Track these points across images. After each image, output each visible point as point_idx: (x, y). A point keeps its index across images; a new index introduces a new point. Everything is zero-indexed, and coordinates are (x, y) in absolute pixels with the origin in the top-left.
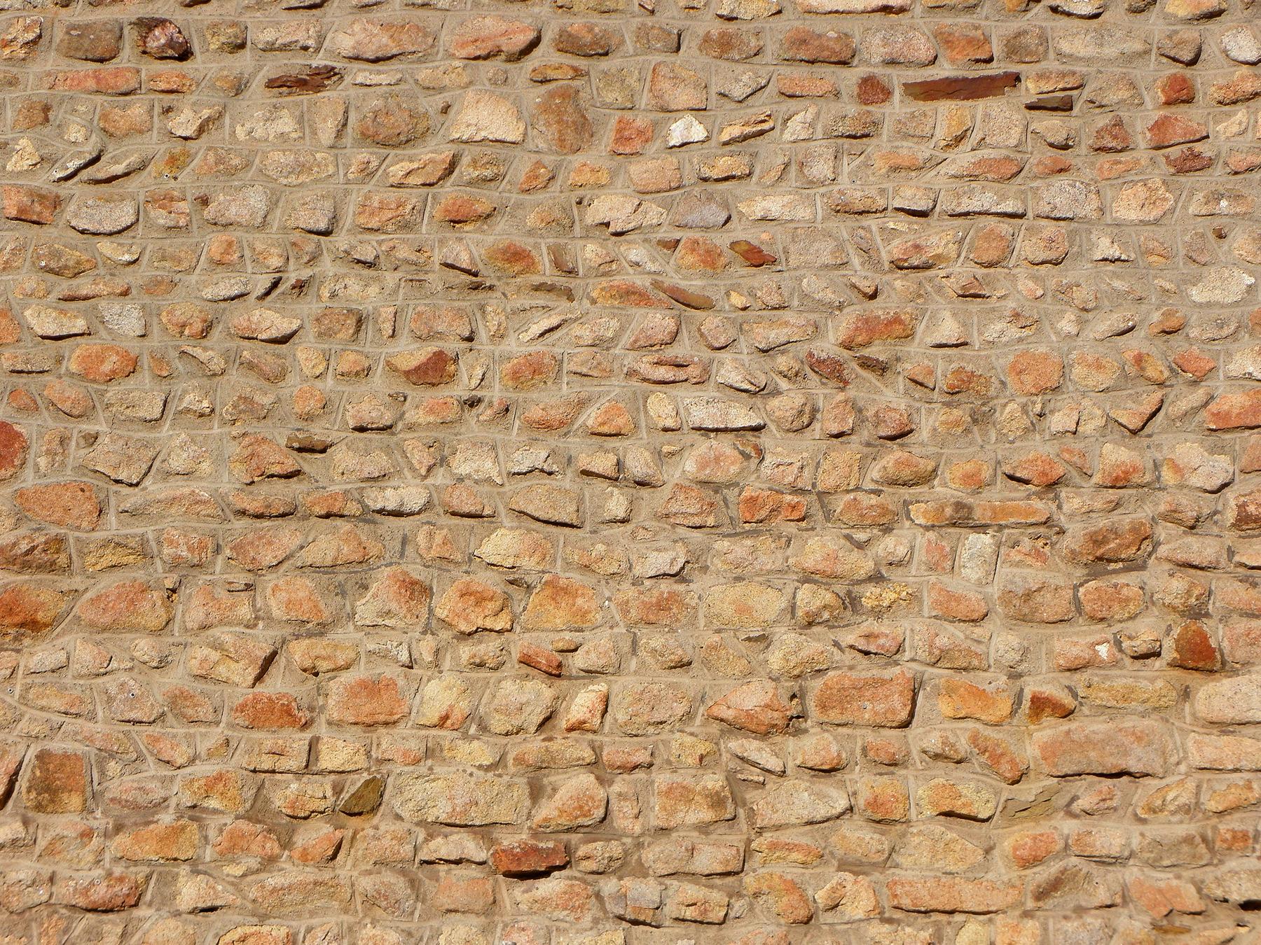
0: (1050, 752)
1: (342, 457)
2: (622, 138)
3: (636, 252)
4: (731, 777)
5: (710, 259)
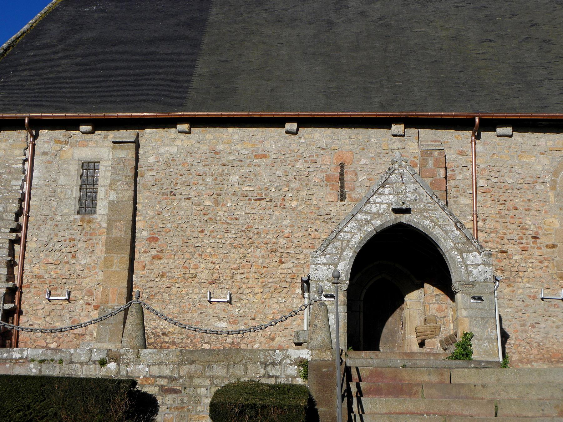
0: (265, 272)
1: (192, 241)
2: (222, 205)
3: (224, 218)
4: (232, 274)
5: (232, 219)
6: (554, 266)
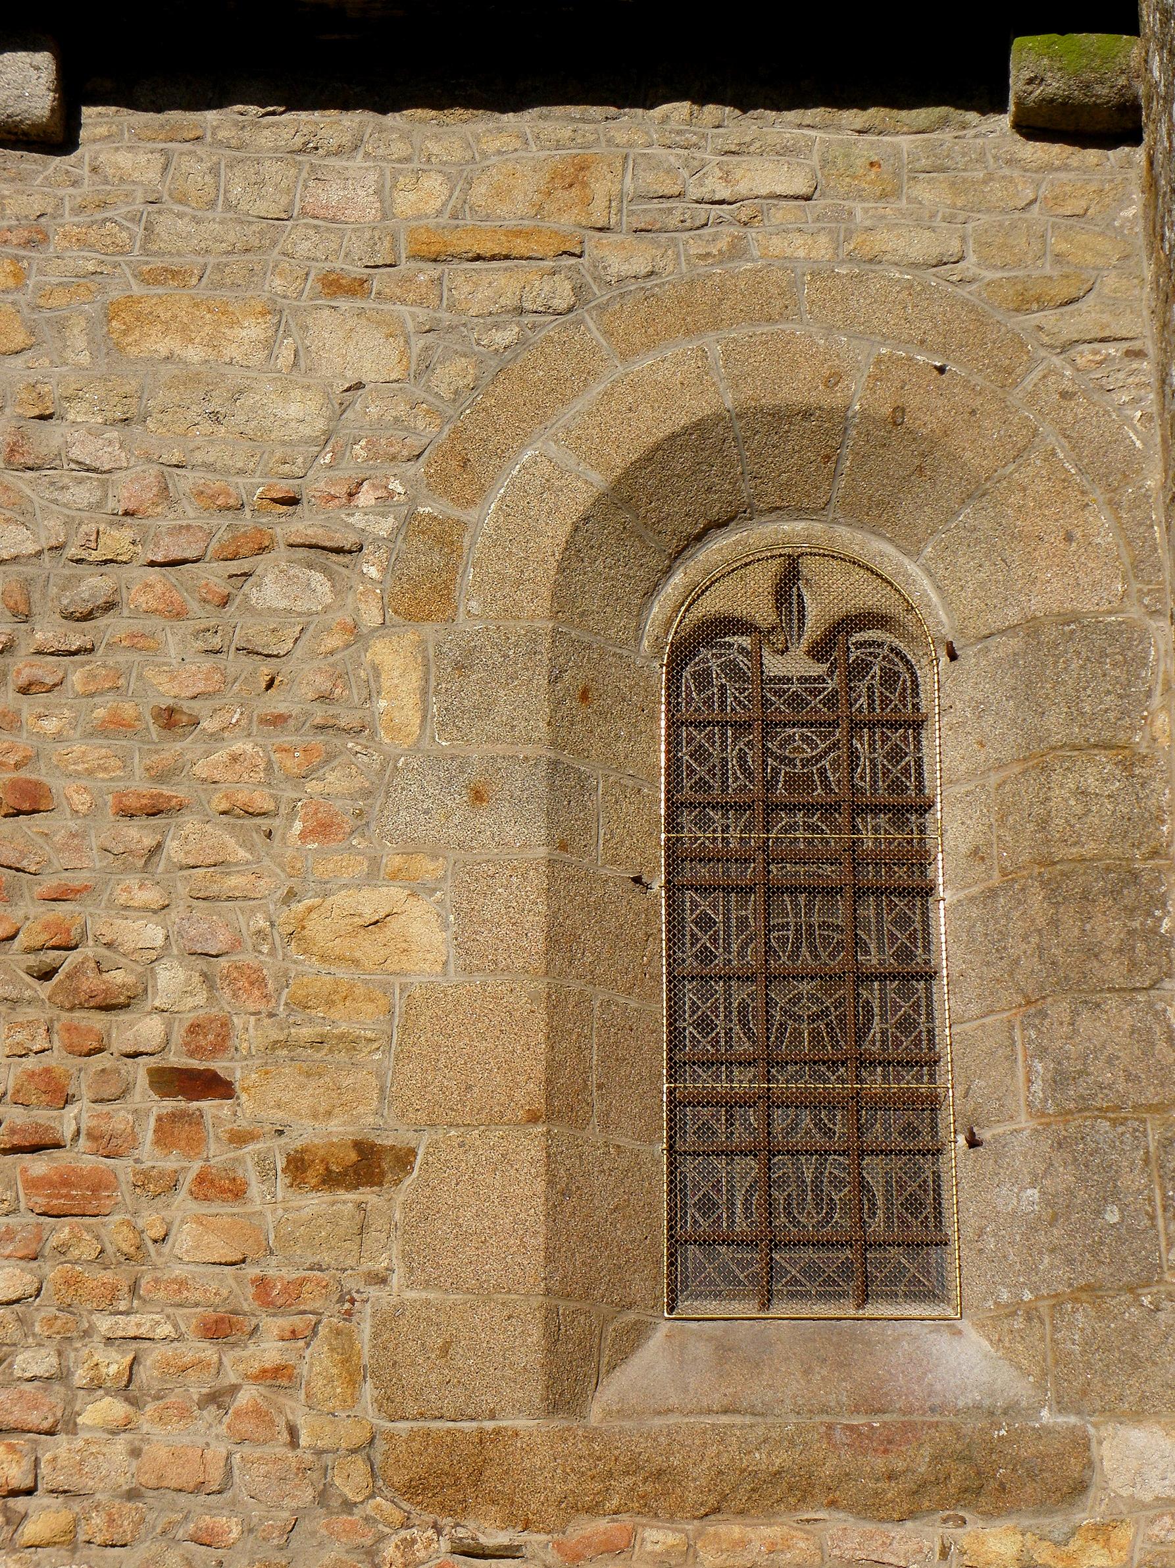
6: (353, 1375)
